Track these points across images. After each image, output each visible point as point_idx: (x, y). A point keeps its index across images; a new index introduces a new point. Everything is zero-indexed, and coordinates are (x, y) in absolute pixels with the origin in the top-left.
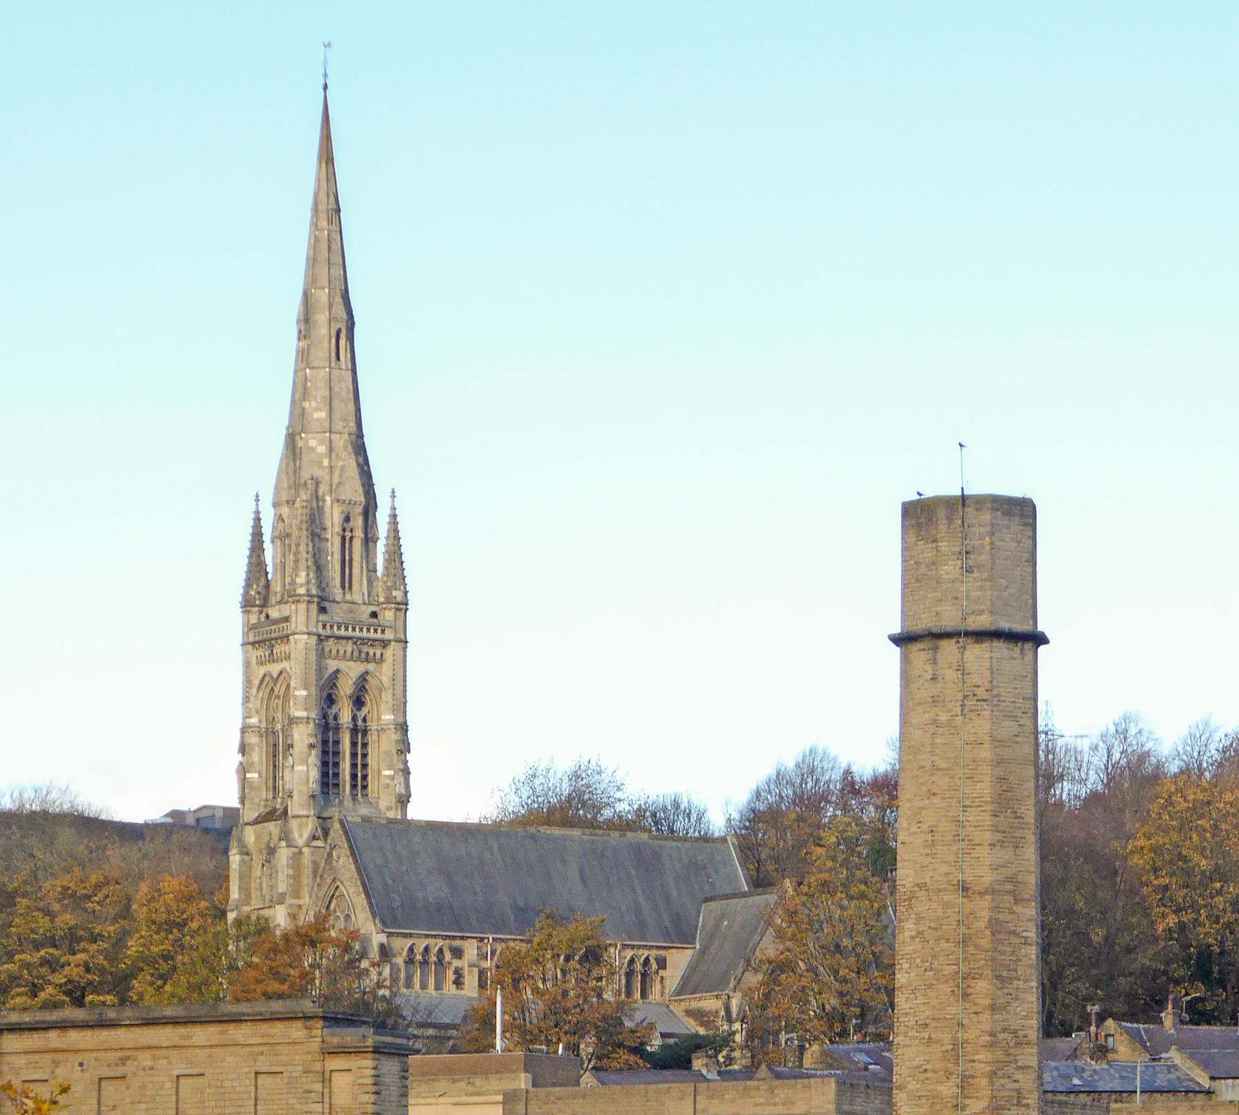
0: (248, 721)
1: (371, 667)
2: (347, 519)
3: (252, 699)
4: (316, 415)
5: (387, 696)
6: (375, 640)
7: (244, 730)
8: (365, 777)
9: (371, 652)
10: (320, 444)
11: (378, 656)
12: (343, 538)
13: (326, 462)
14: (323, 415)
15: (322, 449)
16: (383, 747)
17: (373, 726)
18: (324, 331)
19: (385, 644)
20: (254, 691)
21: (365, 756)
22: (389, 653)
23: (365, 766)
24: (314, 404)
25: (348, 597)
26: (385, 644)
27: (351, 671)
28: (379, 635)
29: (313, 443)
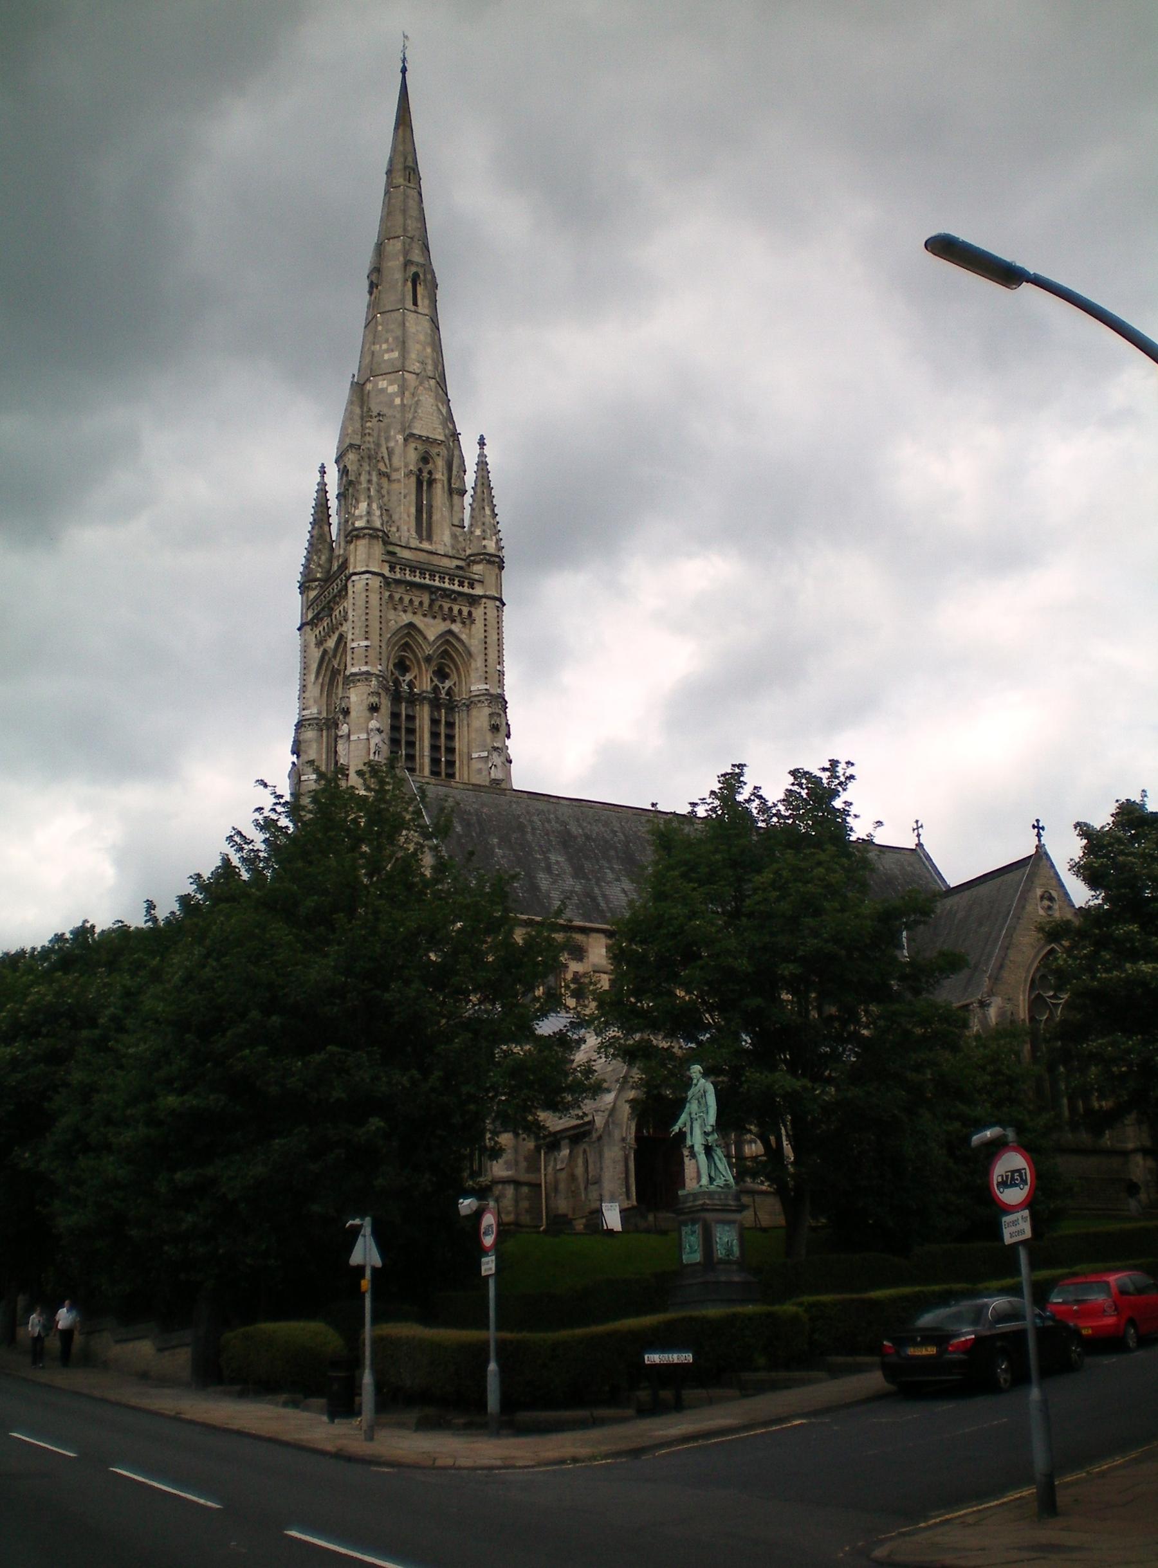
0: (305, 713)
2: (425, 459)
3: (310, 687)
4: (386, 357)
5: (478, 663)
6: (460, 594)
7: (299, 726)
8: (451, 764)
9: (456, 608)
10: (391, 383)
11: (465, 613)
12: (419, 483)
13: (398, 401)
14: (396, 354)
15: (393, 389)
16: (476, 724)
17: (461, 696)
18: (398, 276)
19: (473, 600)
20: (312, 677)
21: (450, 737)
22: (478, 613)
23: (451, 750)
24: (384, 346)
25: (426, 545)
26: (473, 600)
27: (433, 629)
28: (466, 590)
29: (383, 384)
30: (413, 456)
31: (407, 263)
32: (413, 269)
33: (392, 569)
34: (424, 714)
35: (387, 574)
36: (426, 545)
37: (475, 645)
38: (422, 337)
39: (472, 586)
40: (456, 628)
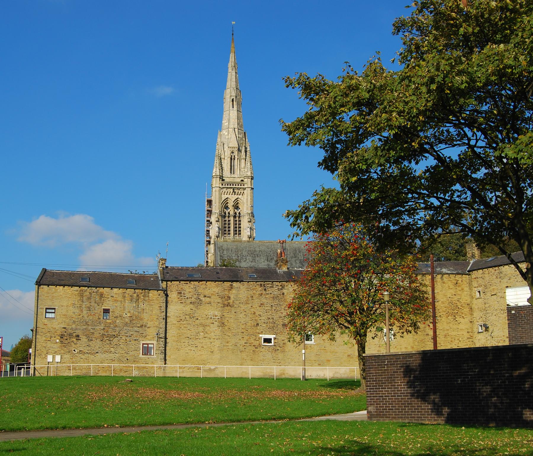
1: (240, 197)
12: (231, 159)
14: (227, 124)
15: (226, 134)
19: (244, 189)
22: (245, 191)
25: (233, 176)
26: (244, 189)
27: (232, 198)
28: (242, 187)
29: (224, 132)
30: (229, 152)
31: (231, 96)
32: (232, 98)
33: (222, 185)
34: (232, 219)
35: (221, 186)
36: (233, 176)
37: (245, 201)
38: (234, 117)
39: (244, 185)
40: (240, 197)
